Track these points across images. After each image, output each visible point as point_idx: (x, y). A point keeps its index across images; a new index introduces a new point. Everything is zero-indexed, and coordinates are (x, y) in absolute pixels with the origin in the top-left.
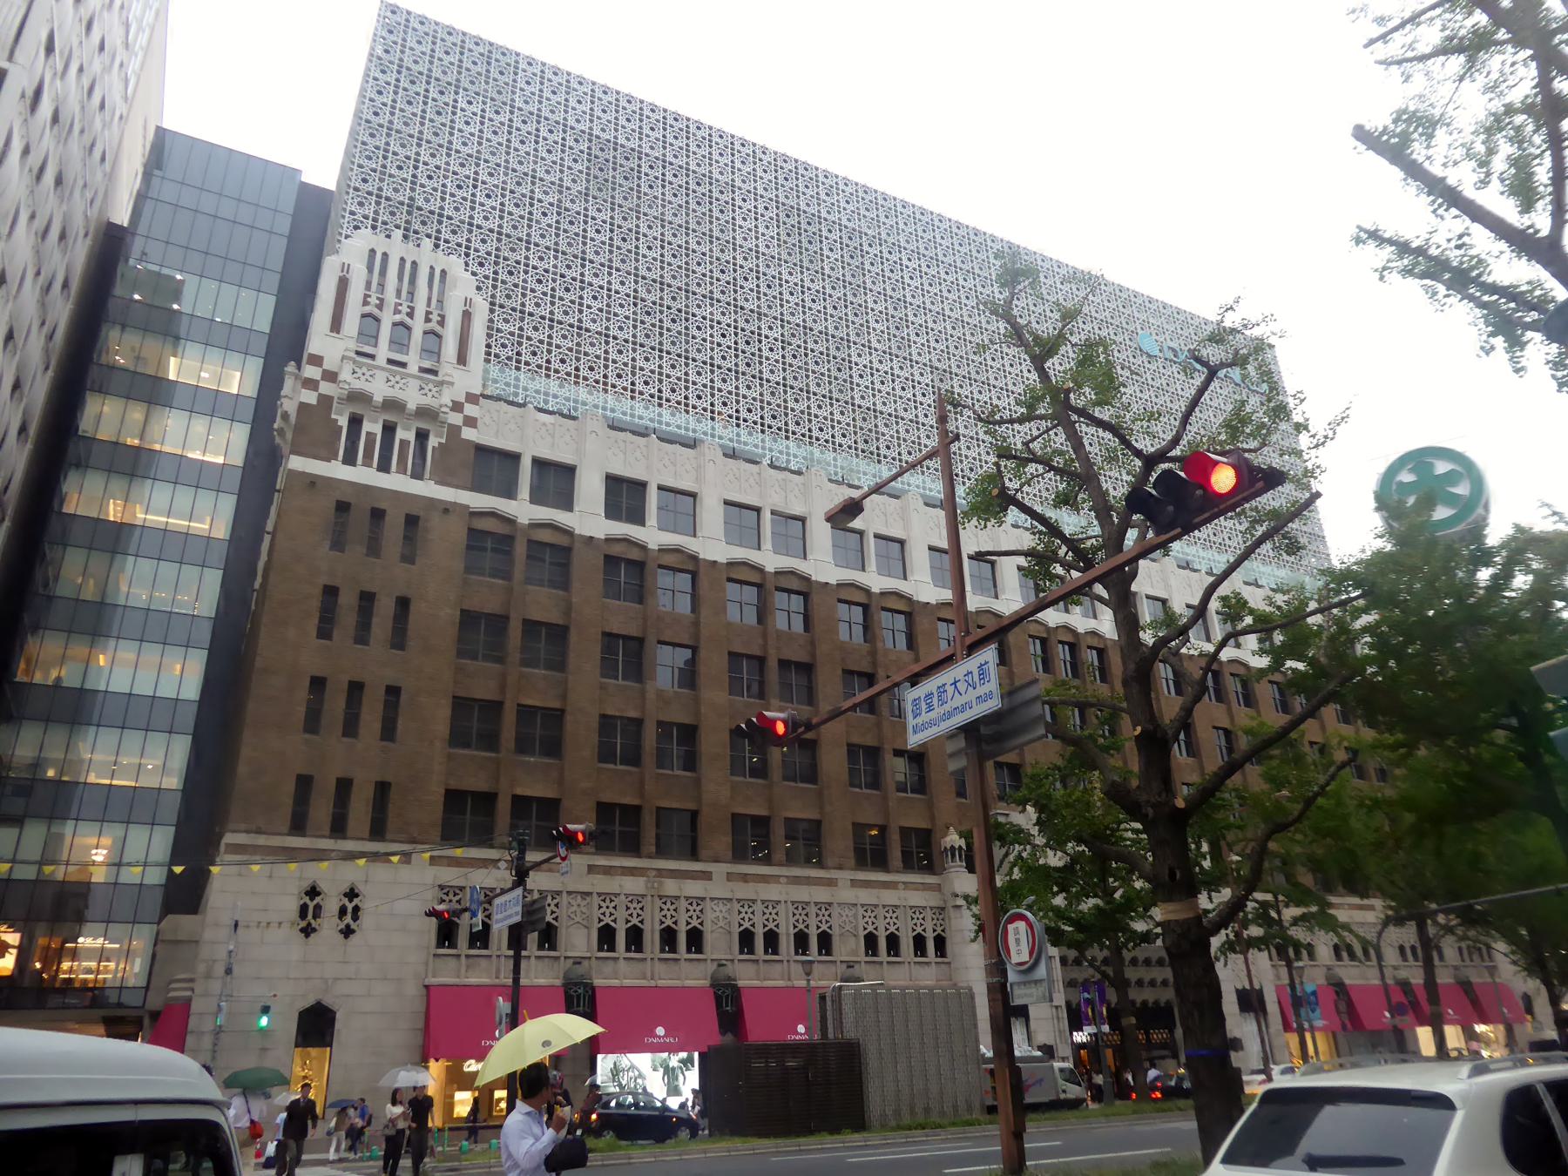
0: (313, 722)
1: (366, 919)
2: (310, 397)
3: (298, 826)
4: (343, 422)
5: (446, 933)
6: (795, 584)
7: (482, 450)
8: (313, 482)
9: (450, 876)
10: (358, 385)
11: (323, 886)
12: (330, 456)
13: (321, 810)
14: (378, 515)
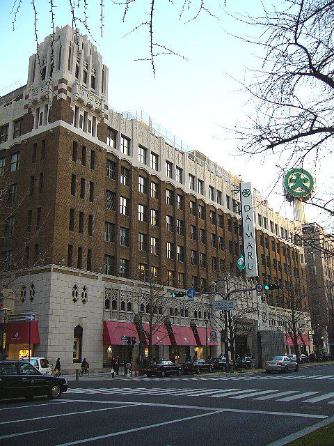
0: (71, 228)
1: (89, 298)
2: (64, 96)
3: (69, 265)
4: (74, 109)
5: (107, 306)
6: (180, 193)
7: (110, 129)
8: (66, 132)
9: (108, 284)
10: (80, 96)
11: (78, 285)
12: (70, 123)
13: (75, 259)
14: (84, 148)
